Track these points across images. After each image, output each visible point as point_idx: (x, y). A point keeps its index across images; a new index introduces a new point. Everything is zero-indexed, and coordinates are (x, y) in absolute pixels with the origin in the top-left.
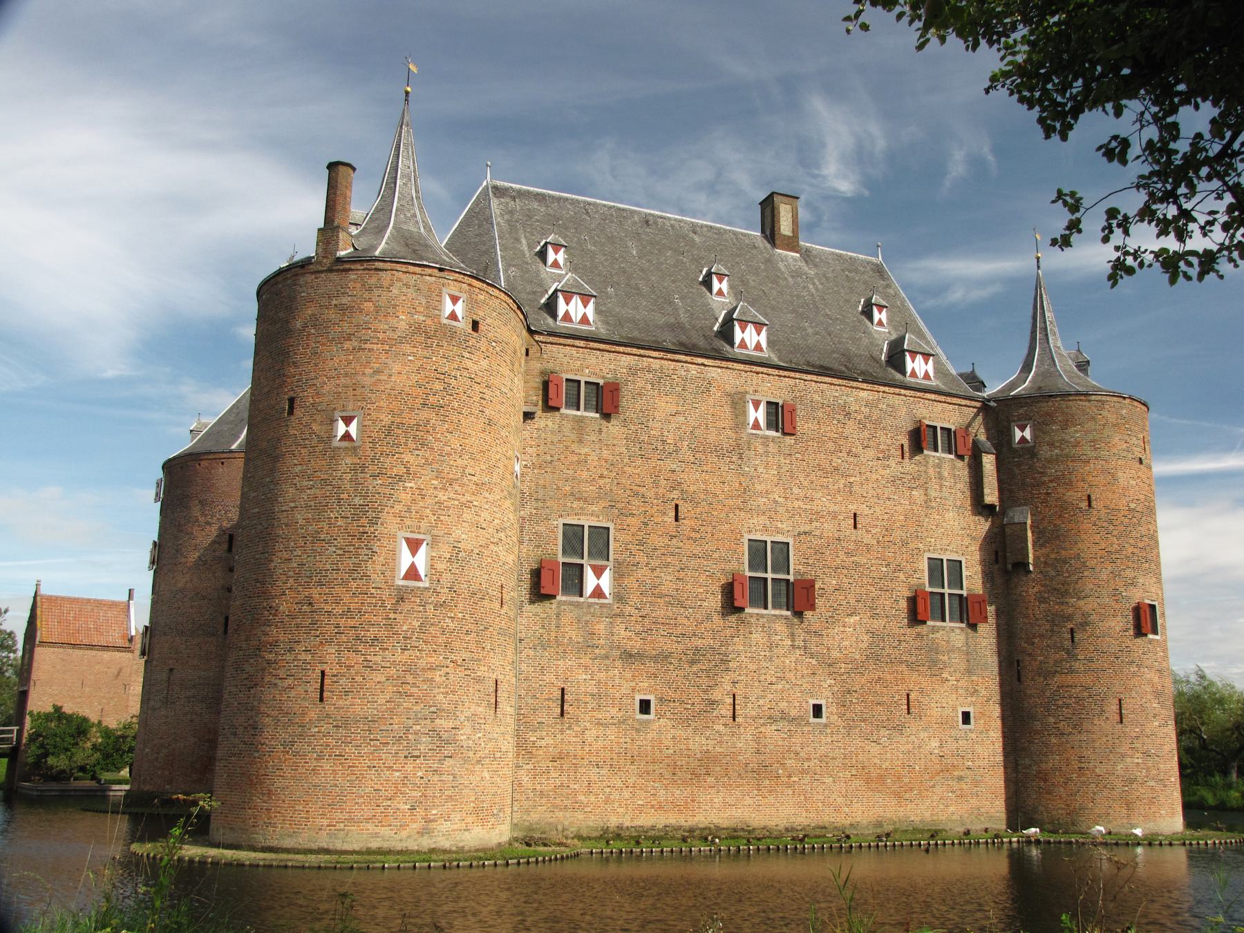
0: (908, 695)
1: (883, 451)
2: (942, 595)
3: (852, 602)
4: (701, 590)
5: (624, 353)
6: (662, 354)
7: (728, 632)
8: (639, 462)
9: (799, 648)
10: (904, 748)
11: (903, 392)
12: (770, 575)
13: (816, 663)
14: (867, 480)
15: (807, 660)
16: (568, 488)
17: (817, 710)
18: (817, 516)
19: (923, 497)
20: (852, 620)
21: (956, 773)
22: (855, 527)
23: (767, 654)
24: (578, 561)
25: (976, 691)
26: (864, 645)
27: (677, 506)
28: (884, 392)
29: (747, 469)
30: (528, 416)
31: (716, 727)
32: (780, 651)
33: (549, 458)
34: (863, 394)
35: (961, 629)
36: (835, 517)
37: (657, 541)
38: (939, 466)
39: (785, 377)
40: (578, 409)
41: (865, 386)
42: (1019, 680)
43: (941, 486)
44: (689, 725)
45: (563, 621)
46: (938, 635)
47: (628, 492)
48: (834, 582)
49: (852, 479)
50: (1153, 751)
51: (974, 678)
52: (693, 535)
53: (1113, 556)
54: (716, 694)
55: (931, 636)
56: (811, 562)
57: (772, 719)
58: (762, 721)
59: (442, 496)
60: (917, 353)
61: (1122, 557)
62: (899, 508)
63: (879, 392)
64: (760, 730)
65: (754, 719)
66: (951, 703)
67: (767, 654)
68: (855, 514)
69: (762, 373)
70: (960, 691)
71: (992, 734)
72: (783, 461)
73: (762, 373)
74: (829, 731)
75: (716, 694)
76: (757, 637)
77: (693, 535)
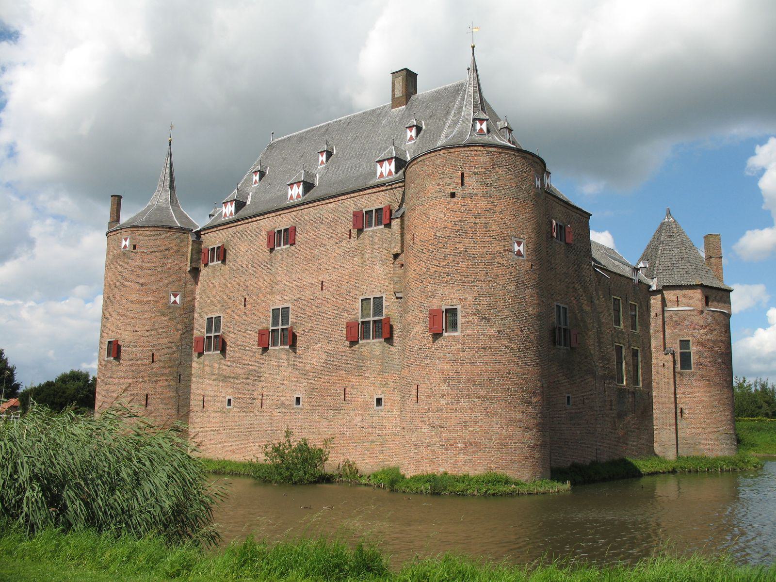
0: (345, 389)
1: (339, 238)
4: (252, 341)
5: (229, 227)
7: (261, 361)
8: (233, 280)
10: (341, 422)
13: (298, 374)
17: (298, 400)
18: (303, 288)
20: (317, 346)
22: (322, 289)
25: (386, 383)
27: (245, 299)
28: (341, 200)
29: (274, 270)
32: (282, 369)
33: (204, 288)
34: (330, 205)
35: (380, 343)
37: (237, 319)
39: (292, 212)
41: (331, 200)
43: (372, 250)
46: (364, 349)
48: (310, 325)
50: (436, 423)
52: (250, 312)
53: (422, 278)
54: (255, 395)
55: (361, 350)
56: (299, 315)
59: (118, 322)
60: (383, 161)
61: (427, 276)
63: (339, 201)
66: (370, 392)
69: (282, 214)
71: (395, 412)
72: (289, 261)
73: (282, 214)
74: (302, 412)
75: (255, 395)
76: (274, 362)
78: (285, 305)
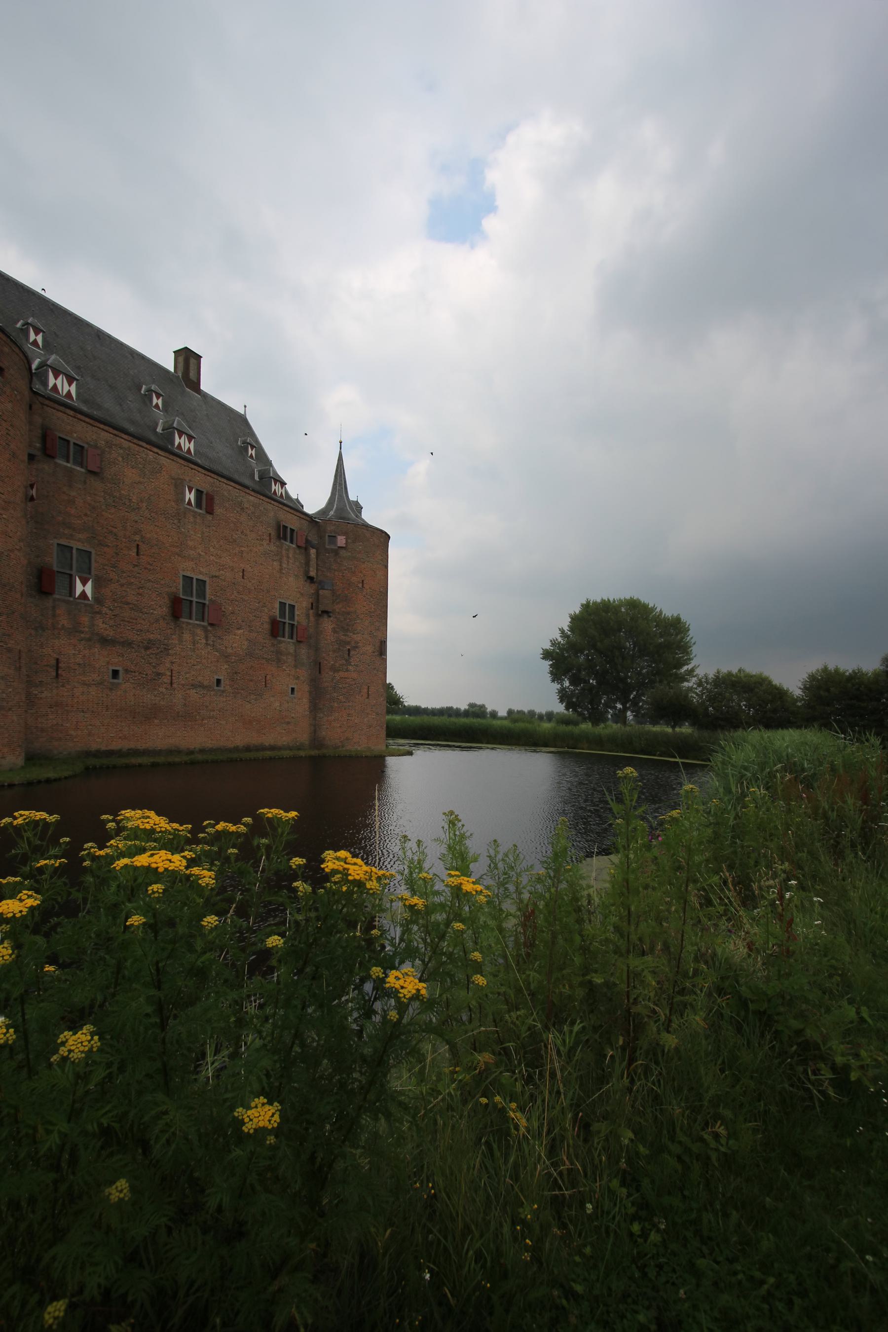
0: (266, 677)
1: (260, 536)
2: (285, 623)
3: (240, 621)
4: (153, 603)
6: (130, 438)
9: (209, 645)
11: (273, 502)
12: (194, 599)
14: (251, 550)
15: (214, 653)
16: (61, 519)
17: (219, 682)
19: (279, 567)
21: (287, 720)
23: (192, 647)
24: (68, 572)
26: (244, 647)
28: (262, 500)
29: (183, 530)
30: (31, 457)
31: (161, 689)
34: (251, 498)
36: (232, 570)
38: (287, 550)
39: (208, 476)
40: (68, 461)
41: (252, 493)
42: (320, 672)
43: (288, 562)
44: (144, 688)
45: (58, 612)
47: (105, 530)
49: (243, 549)
51: (298, 670)
52: (149, 567)
56: (218, 594)
57: (194, 686)
58: (187, 687)
62: (266, 570)
64: (187, 692)
65: (183, 685)
67: (192, 647)
68: (243, 570)
69: (195, 469)
70: (291, 677)
72: (205, 530)
74: (225, 695)
75: (161, 669)
76: (187, 636)
77: (149, 567)
78: (201, 577)
